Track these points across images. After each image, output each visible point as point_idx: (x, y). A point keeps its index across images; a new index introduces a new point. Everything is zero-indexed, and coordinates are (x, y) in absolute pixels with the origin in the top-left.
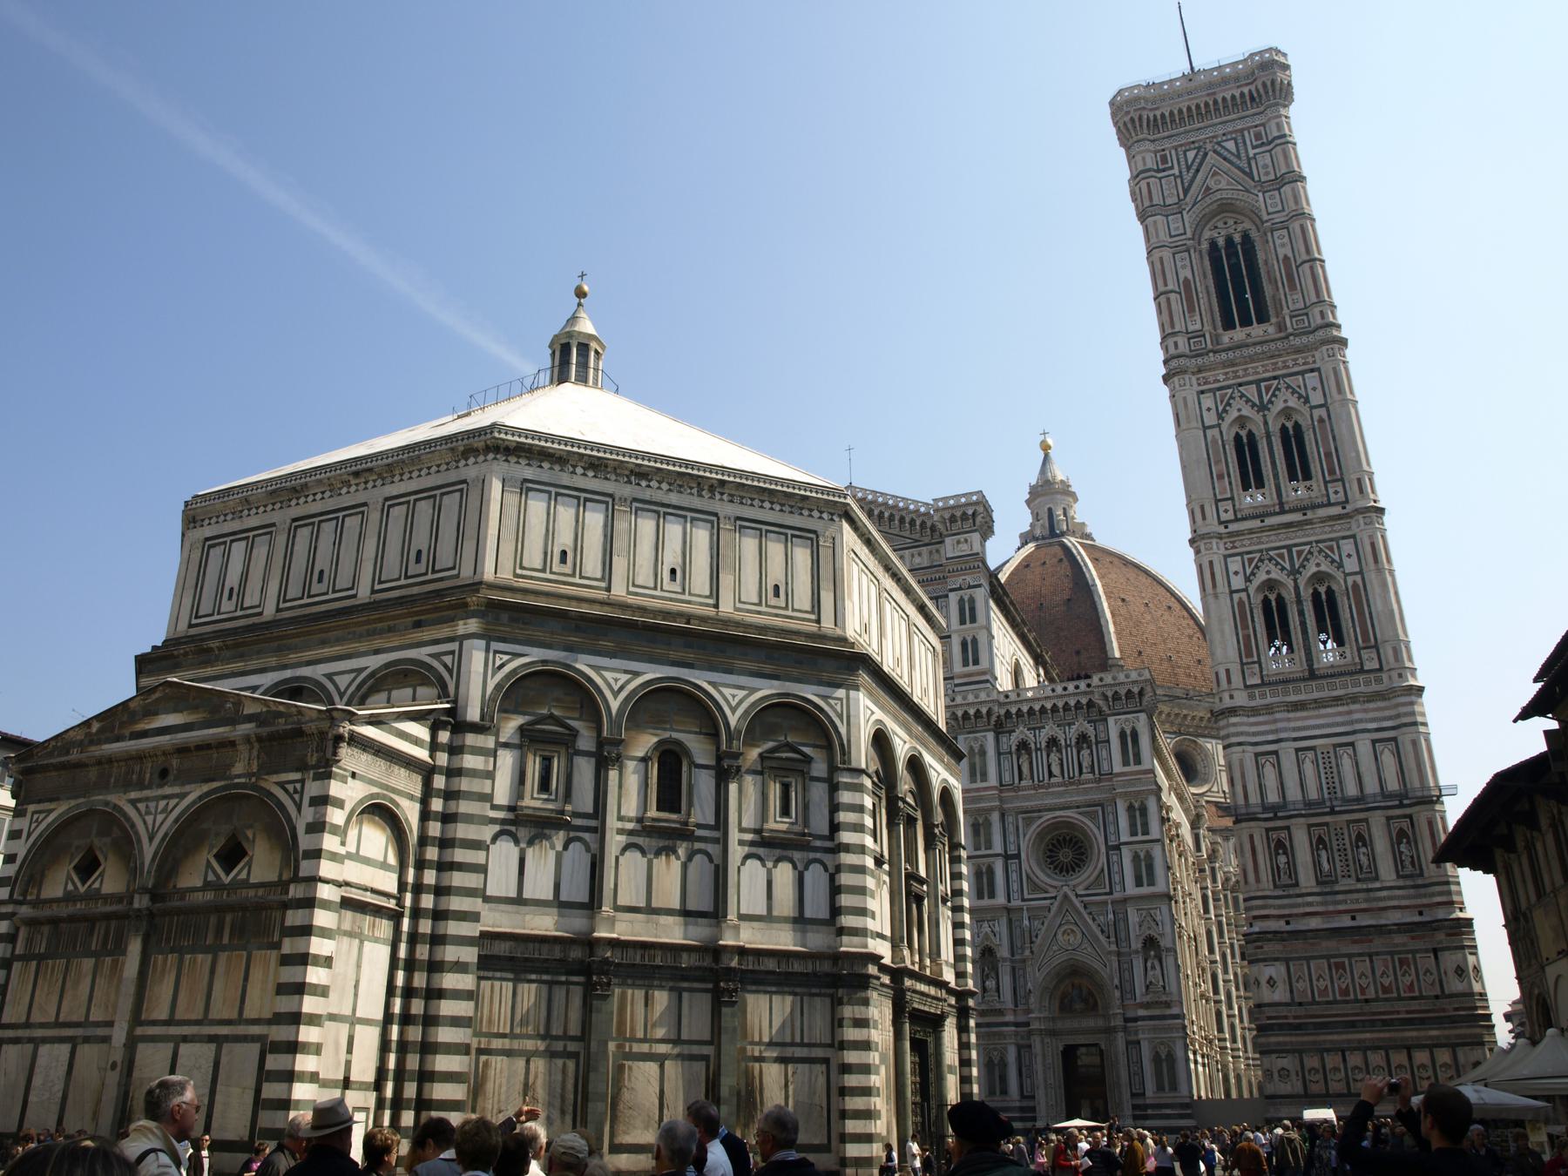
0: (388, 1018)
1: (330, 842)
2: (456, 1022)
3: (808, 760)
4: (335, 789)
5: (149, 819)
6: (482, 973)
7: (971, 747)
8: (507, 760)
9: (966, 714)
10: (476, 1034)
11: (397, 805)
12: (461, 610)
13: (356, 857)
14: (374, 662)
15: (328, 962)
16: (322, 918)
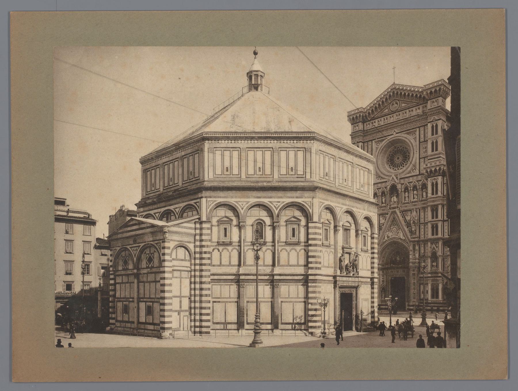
0: (191, 295)
1: (167, 257)
2: (206, 295)
3: (300, 220)
4: (166, 245)
5: (134, 252)
6: (212, 284)
7: (433, 182)
8: (215, 229)
9: (431, 171)
10: (213, 298)
11: (186, 245)
12: (200, 190)
13: (176, 259)
14: (182, 205)
15: (170, 285)
16: (166, 275)
